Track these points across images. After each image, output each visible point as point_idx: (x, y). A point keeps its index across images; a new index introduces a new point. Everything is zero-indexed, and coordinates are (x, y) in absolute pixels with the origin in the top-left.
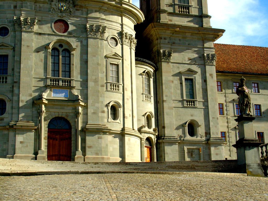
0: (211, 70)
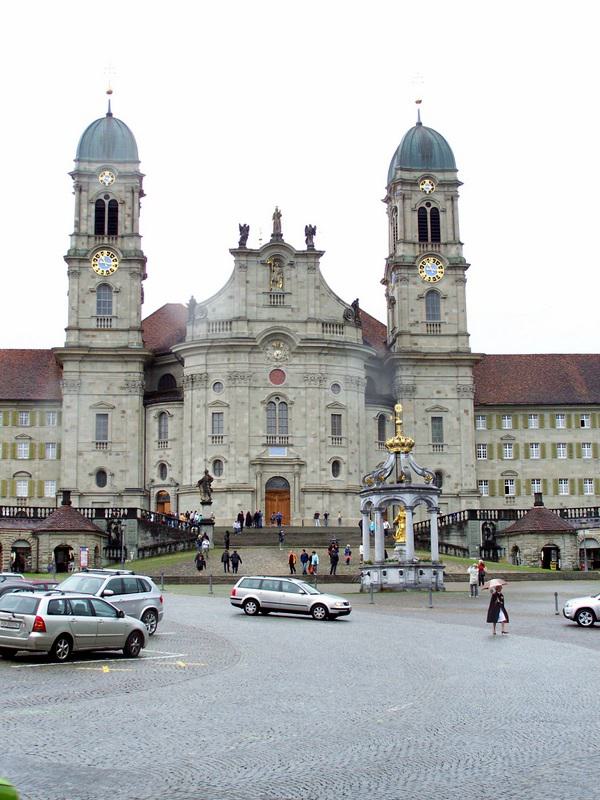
0: (469, 405)
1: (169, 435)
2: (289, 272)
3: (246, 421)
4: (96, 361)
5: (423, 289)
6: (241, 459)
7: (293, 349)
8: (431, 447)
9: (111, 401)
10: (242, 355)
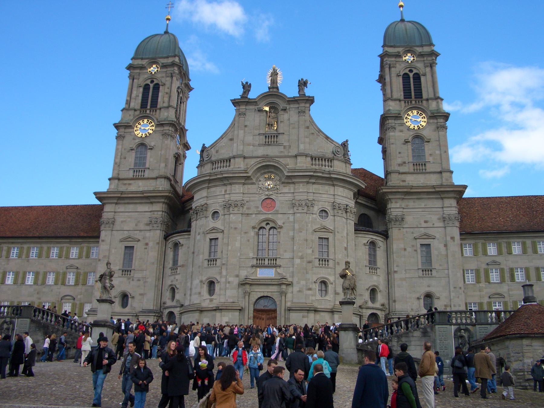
0: (456, 232)
1: (179, 261)
2: (284, 116)
3: (238, 244)
4: (128, 203)
5: (409, 136)
6: (231, 279)
7: (283, 180)
8: (420, 271)
9: (138, 235)
10: (237, 186)
